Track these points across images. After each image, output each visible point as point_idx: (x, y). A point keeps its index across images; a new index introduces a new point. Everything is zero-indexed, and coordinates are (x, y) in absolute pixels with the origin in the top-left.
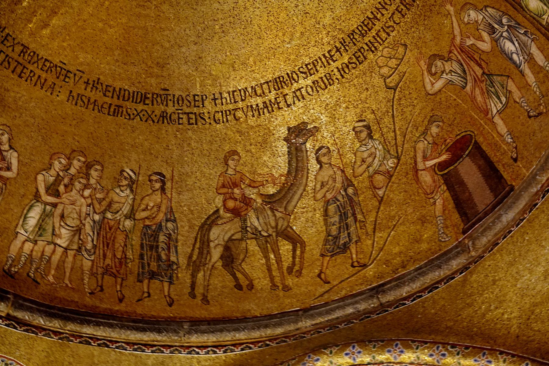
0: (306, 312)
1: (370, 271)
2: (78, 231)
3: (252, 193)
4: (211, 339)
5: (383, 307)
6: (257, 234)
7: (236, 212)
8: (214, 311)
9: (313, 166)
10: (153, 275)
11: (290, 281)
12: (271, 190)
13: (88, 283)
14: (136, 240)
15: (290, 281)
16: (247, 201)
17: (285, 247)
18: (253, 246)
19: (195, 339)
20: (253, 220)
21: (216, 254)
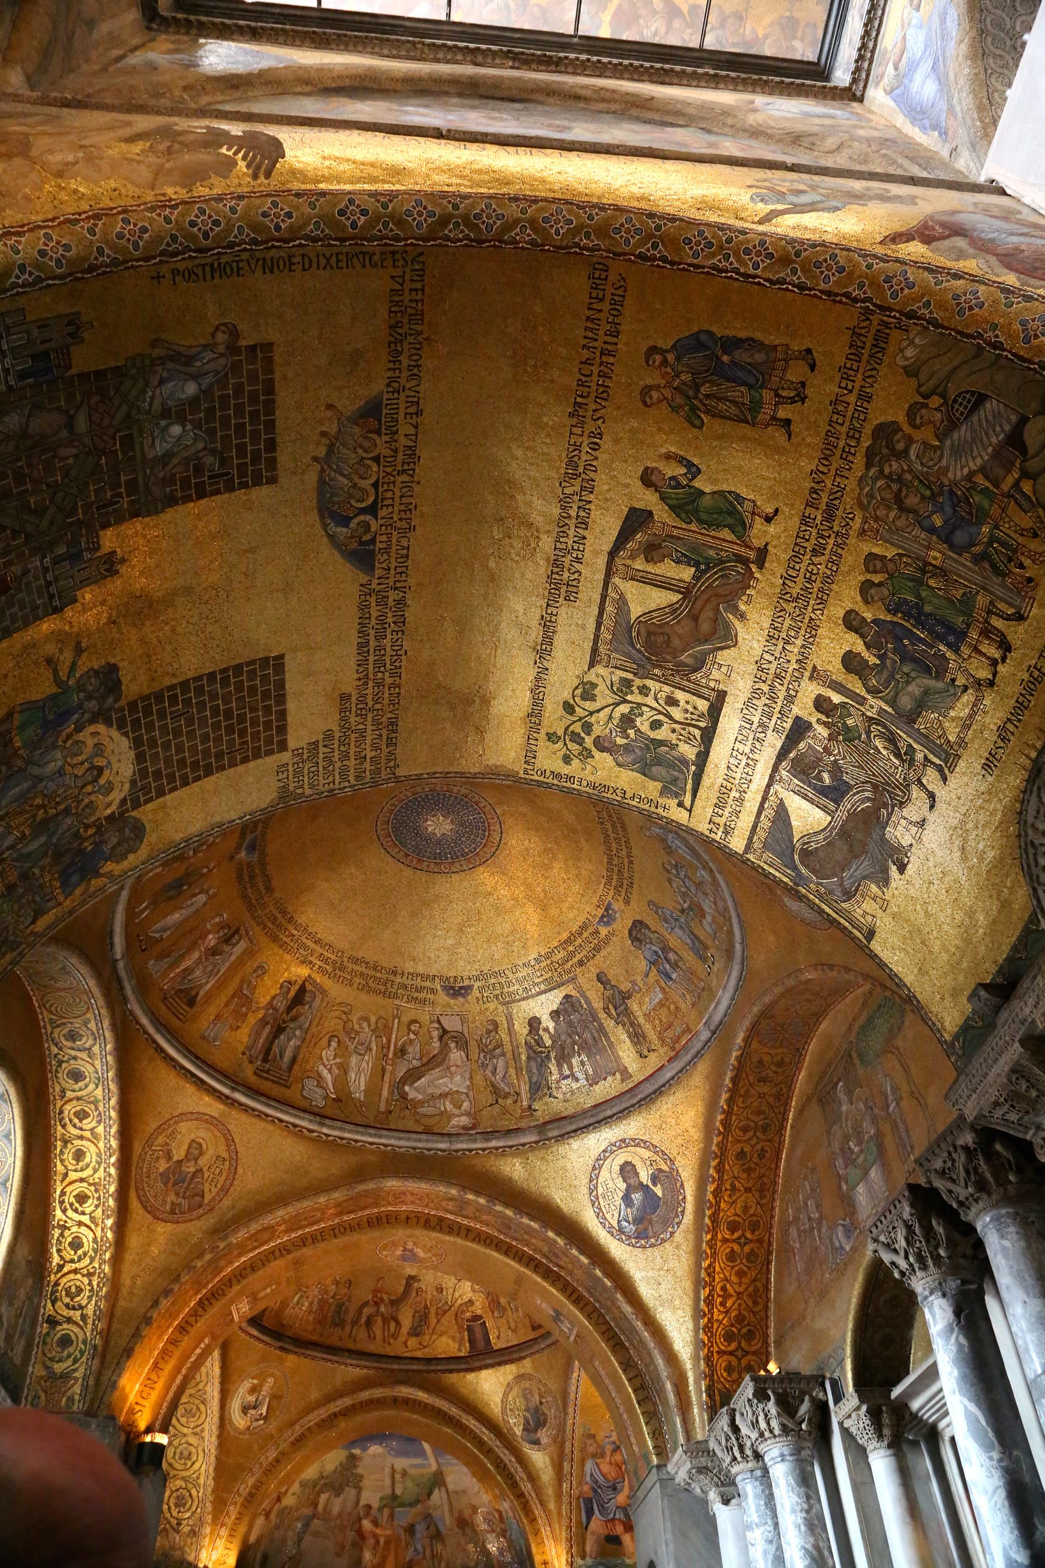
0: (397, 1358)
1: (426, 1350)
2: (311, 1304)
3: (385, 1297)
4: (354, 1362)
5: (429, 1372)
6: (383, 1315)
7: (376, 1303)
8: (358, 1347)
9: (414, 1294)
10: (336, 1325)
11: (392, 1341)
12: (393, 1298)
13: (311, 1327)
14: (333, 1308)
15: (392, 1341)
16: (382, 1300)
17: (393, 1325)
18: (379, 1319)
19: (349, 1361)
20: (383, 1309)
21: (364, 1319)
